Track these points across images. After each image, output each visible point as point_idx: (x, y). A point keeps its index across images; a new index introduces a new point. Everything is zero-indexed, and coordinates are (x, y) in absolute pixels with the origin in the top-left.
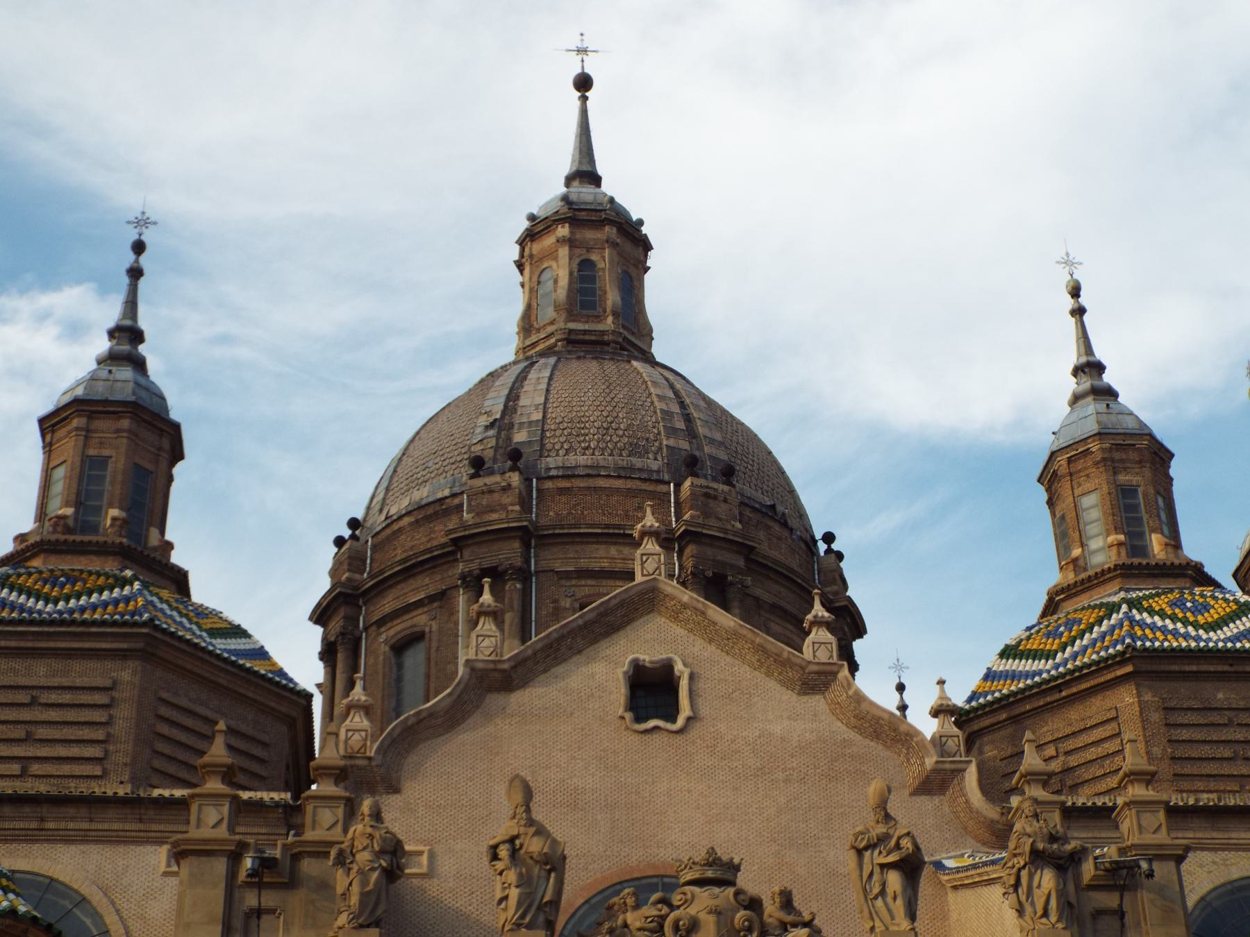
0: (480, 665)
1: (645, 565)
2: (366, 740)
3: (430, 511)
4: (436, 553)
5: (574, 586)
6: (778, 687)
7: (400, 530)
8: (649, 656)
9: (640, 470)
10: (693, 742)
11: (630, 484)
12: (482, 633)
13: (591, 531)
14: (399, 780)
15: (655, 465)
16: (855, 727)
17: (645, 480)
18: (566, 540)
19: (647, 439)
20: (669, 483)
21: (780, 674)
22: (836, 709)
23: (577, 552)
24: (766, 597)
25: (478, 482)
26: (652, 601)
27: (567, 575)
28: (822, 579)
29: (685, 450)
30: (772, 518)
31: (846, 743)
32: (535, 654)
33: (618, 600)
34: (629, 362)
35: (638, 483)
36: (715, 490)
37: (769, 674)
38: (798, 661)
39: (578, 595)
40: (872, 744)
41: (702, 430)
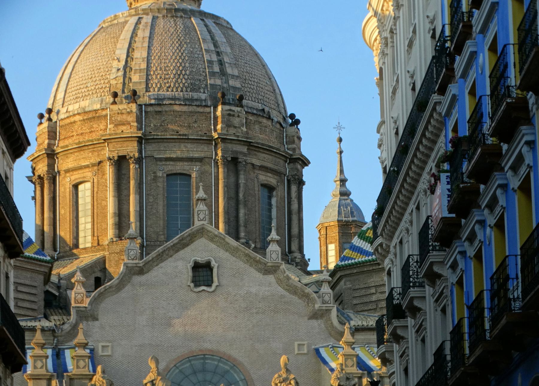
0: (129, 265)
1: (199, 216)
2: (83, 297)
3: (90, 116)
4: (95, 142)
5: (163, 165)
6: (255, 271)
7: (75, 122)
8: (201, 259)
9: (197, 100)
10: (219, 296)
11: (191, 109)
12: (130, 248)
13: (172, 137)
14: (98, 315)
15: (203, 96)
16: (287, 289)
17: (198, 106)
18: (159, 141)
19: (200, 80)
20: (210, 107)
21: (256, 266)
22: (279, 282)
23: (165, 147)
24: (257, 162)
25: (115, 107)
26: (202, 233)
27: (160, 159)
28: (288, 140)
29: (219, 85)
30: (263, 117)
31: (282, 296)
32: (153, 259)
33: (188, 234)
34: (190, 18)
35: (195, 107)
36: (234, 111)
37: (251, 266)
38: (263, 261)
39: (166, 170)
40: (293, 297)
41: (229, 71)
